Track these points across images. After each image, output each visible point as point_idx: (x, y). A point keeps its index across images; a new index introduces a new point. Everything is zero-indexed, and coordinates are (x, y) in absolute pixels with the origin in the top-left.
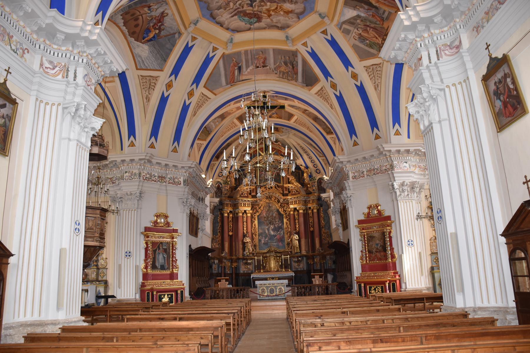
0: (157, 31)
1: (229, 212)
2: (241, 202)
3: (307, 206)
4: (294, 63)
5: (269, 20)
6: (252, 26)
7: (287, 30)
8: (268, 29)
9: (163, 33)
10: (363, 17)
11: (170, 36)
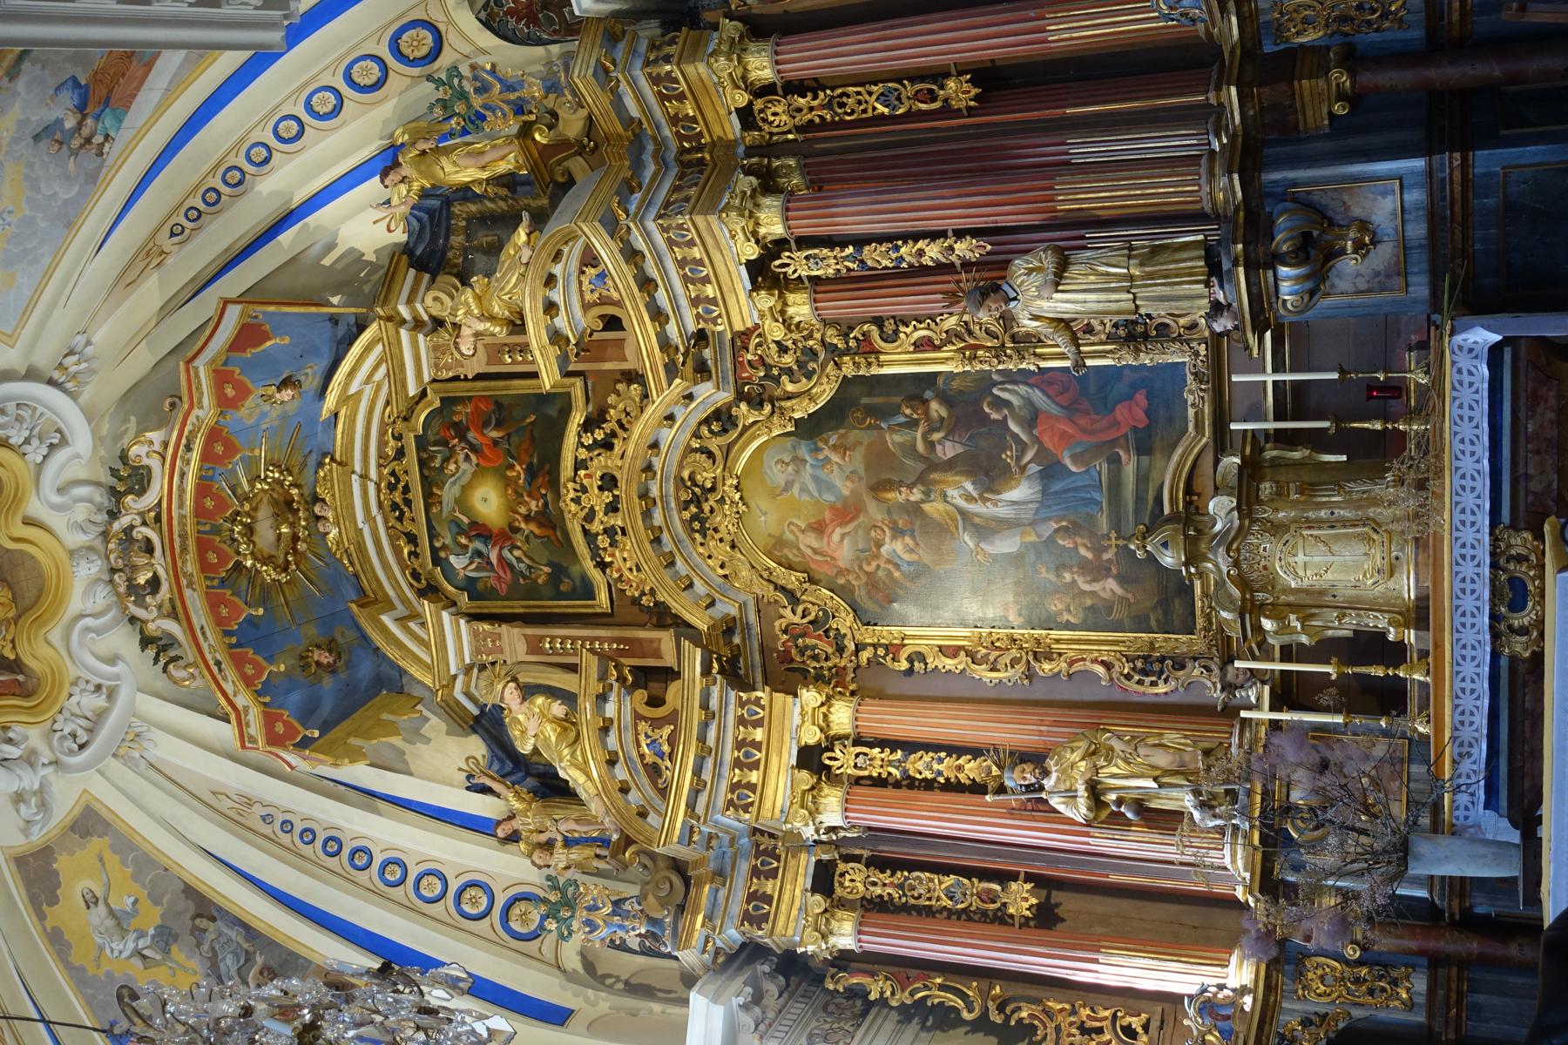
1: (818, 902)
2: (724, 786)
3: (732, 145)
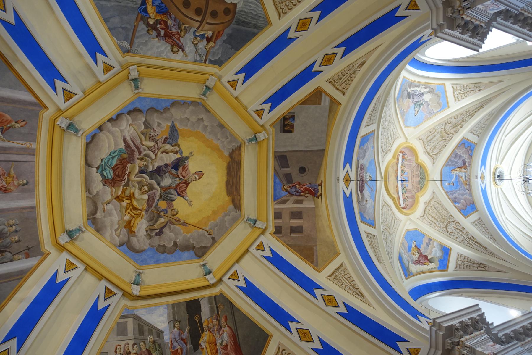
0: (151, 22)
4: (5, 254)
5: (109, 197)
6: (95, 169)
7: (91, 229)
8: (87, 197)
9: (142, 27)
10: (163, 341)
11: (131, 34)
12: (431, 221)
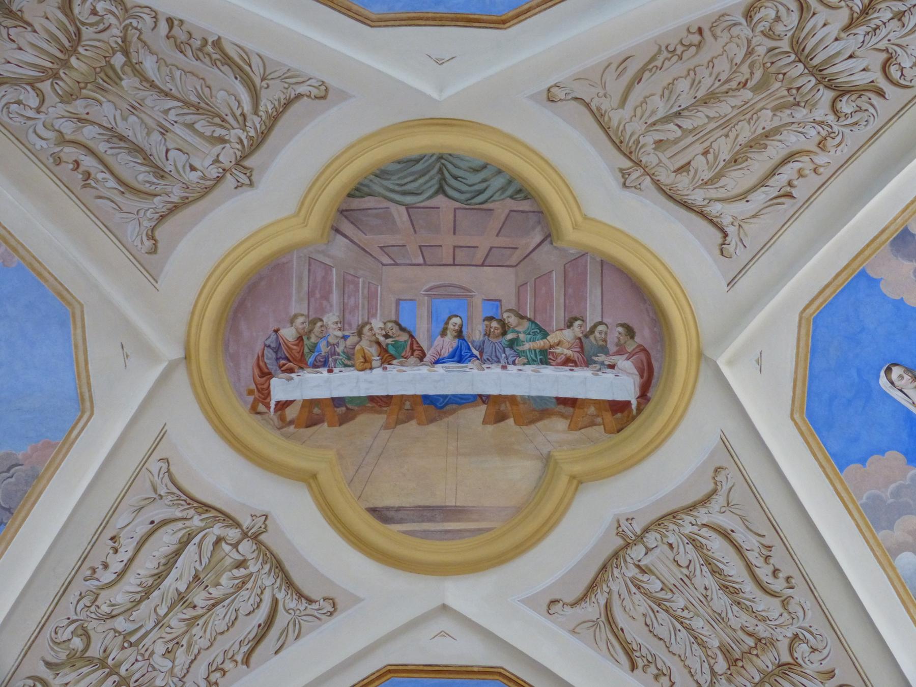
12: (762, 183)
